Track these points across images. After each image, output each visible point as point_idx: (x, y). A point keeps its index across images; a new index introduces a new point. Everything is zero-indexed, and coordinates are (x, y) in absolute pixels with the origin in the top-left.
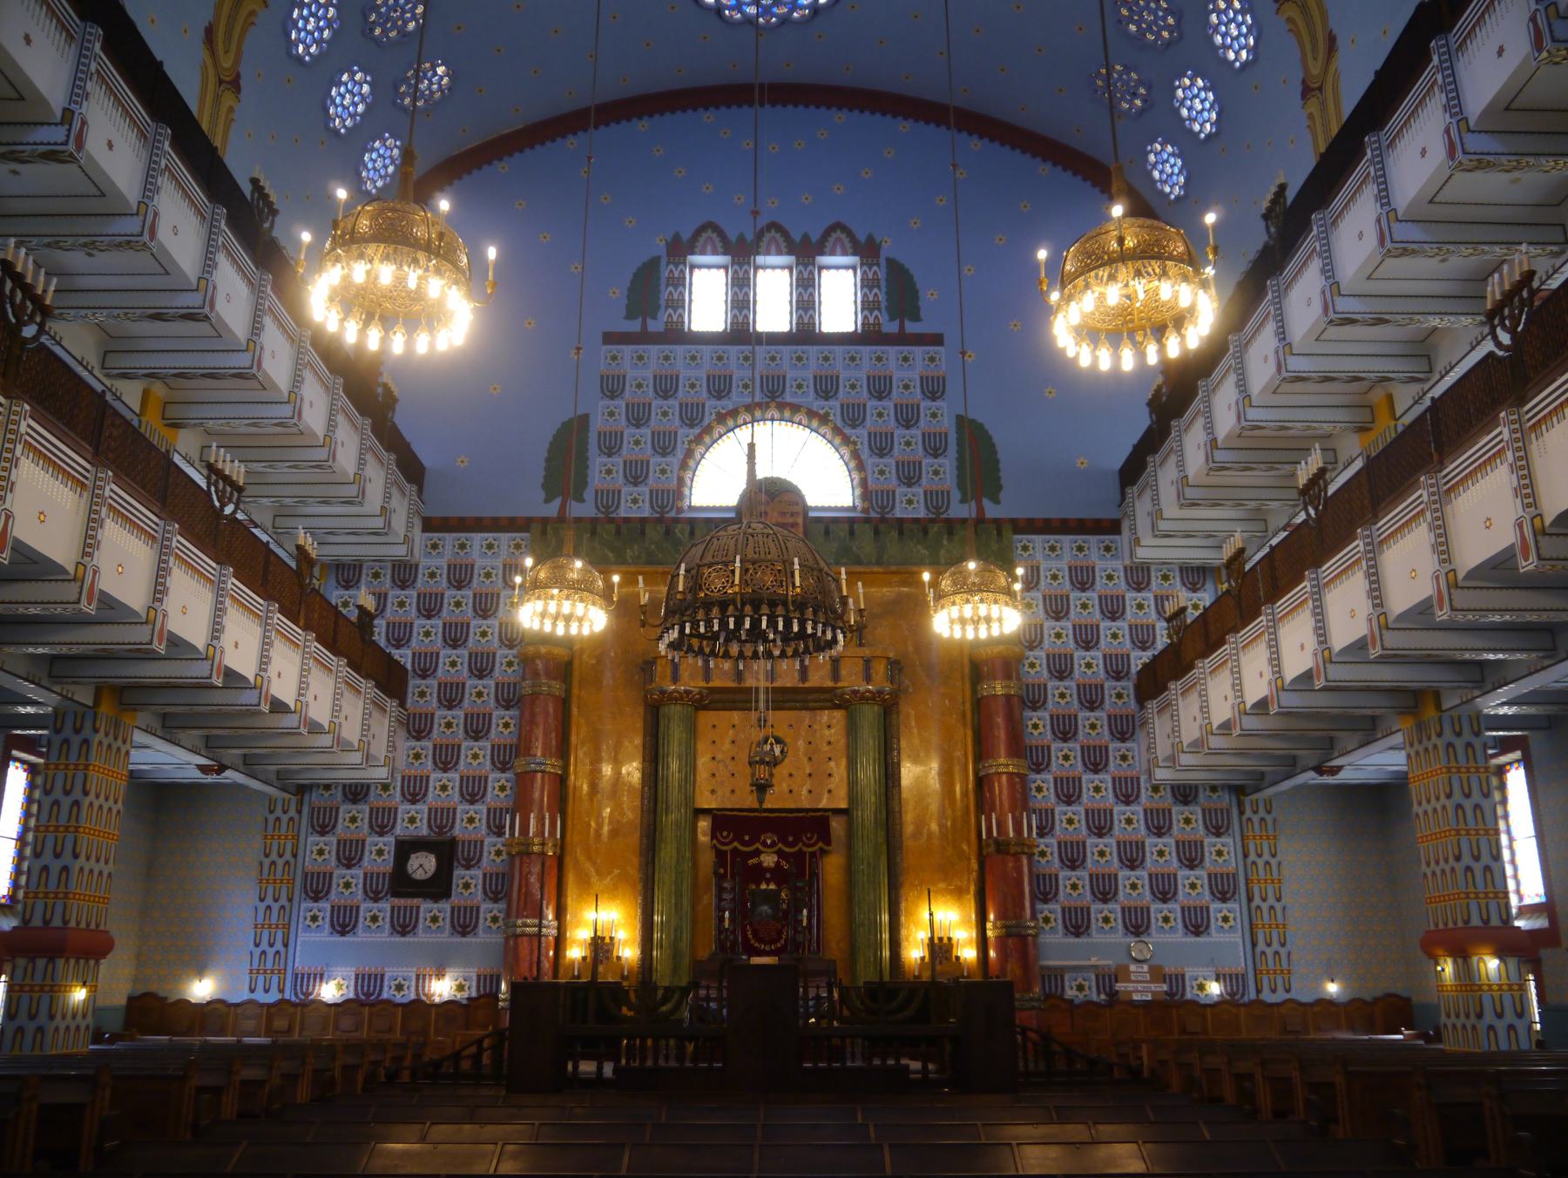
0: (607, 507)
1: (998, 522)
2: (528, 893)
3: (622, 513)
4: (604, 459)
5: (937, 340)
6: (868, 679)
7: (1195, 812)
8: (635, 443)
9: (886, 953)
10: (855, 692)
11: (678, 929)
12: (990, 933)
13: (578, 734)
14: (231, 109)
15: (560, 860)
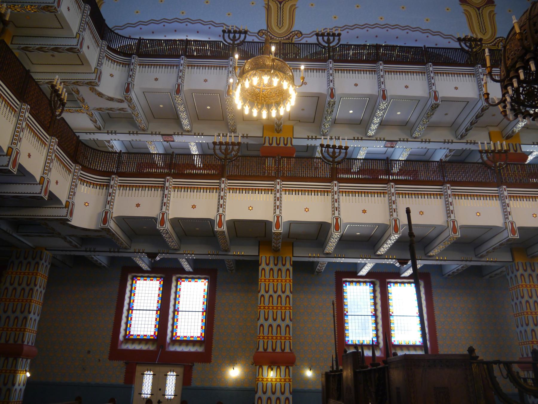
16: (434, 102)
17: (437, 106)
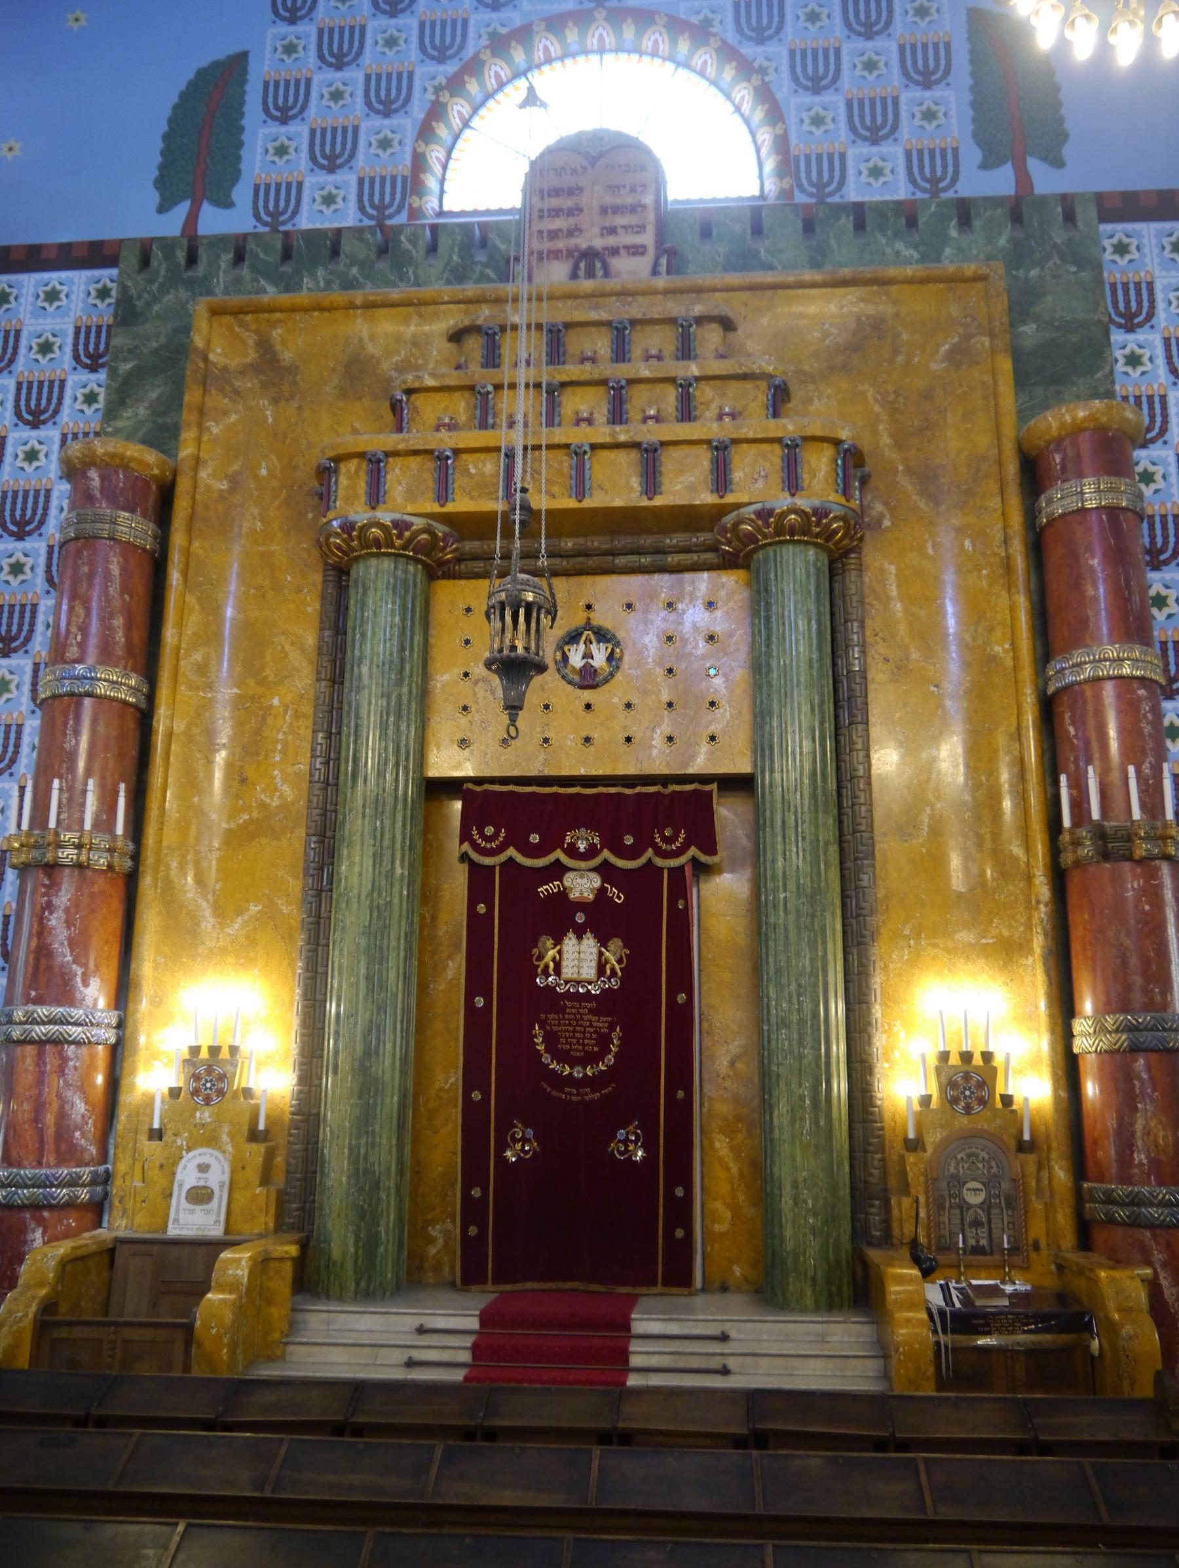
0: (275, 215)
2: (43, 952)
3: (305, 222)
4: (274, 129)
6: (793, 484)
8: (338, 95)
9: (840, 1086)
10: (765, 514)
11: (373, 1029)
12: (1080, 1044)
13: (180, 626)
15: (131, 881)
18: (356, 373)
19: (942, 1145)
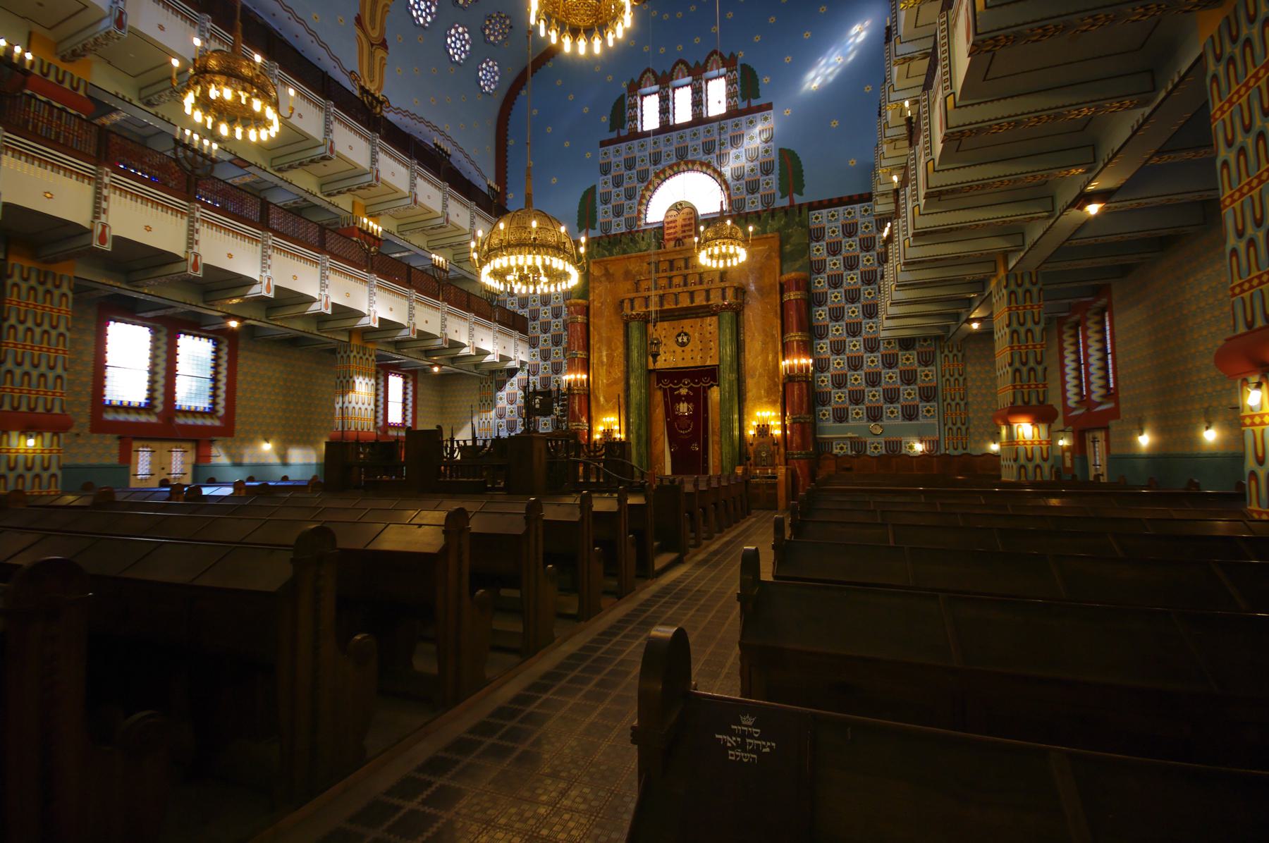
1: (801, 206)
5: (769, 107)
7: (913, 355)
9: (736, 433)
14: (383, 58)
16: (328, 153)
17: (330, 159)
18: (627, 275)
19: (759, 445)
